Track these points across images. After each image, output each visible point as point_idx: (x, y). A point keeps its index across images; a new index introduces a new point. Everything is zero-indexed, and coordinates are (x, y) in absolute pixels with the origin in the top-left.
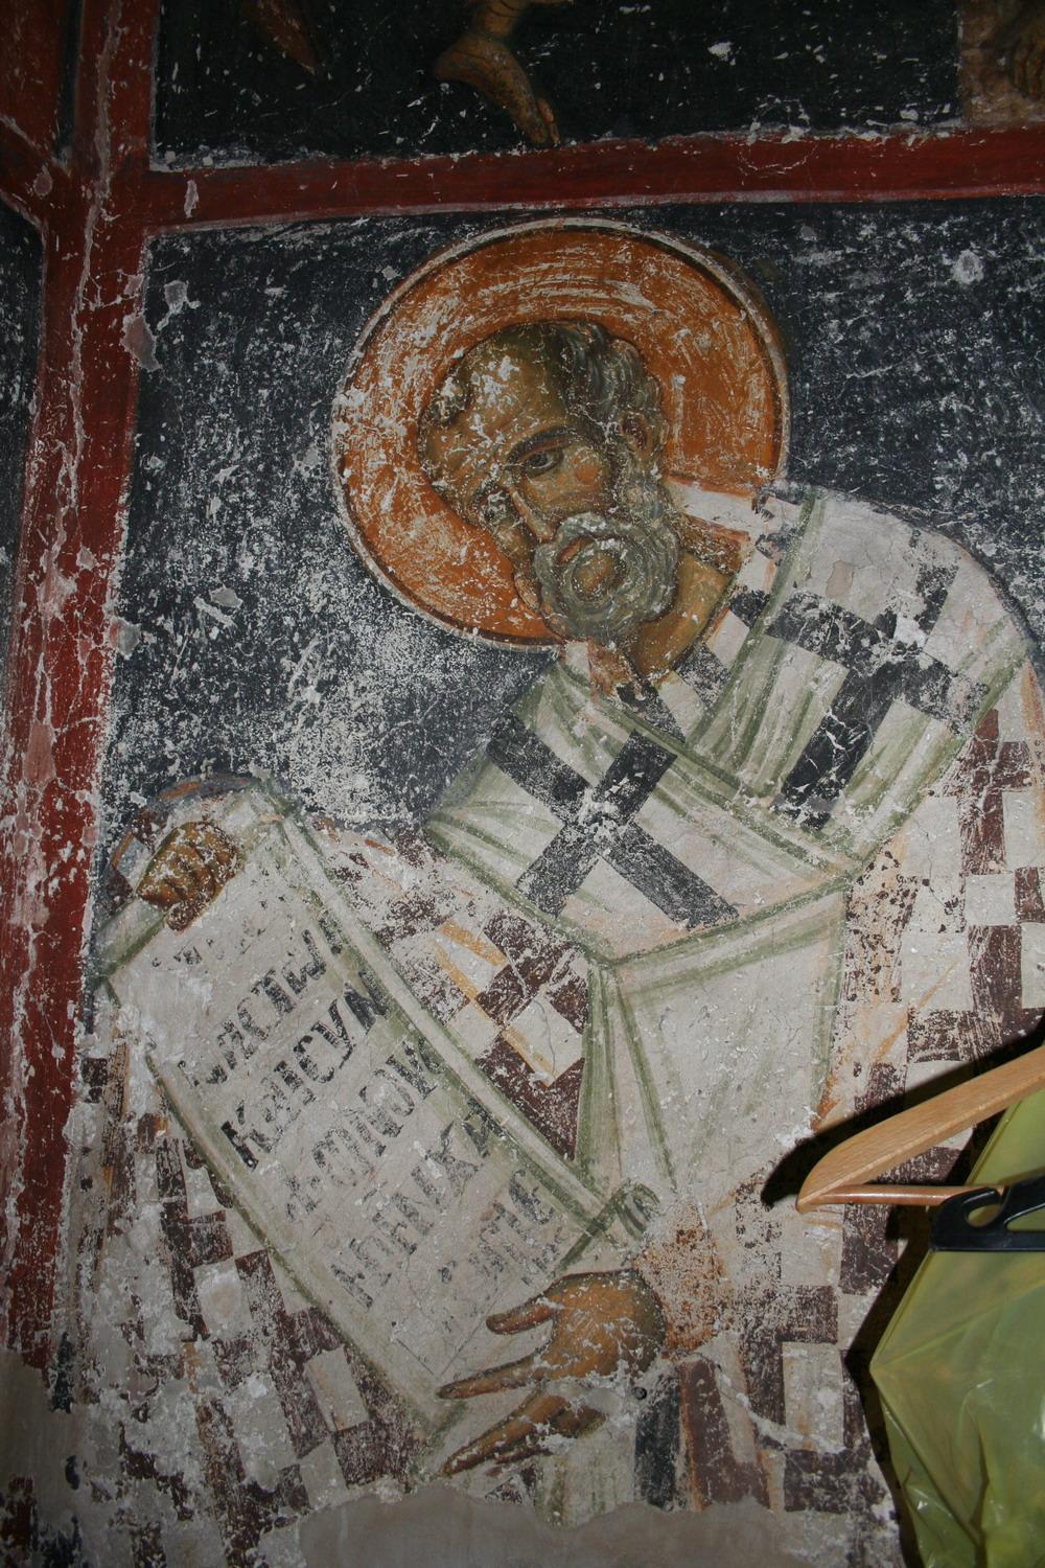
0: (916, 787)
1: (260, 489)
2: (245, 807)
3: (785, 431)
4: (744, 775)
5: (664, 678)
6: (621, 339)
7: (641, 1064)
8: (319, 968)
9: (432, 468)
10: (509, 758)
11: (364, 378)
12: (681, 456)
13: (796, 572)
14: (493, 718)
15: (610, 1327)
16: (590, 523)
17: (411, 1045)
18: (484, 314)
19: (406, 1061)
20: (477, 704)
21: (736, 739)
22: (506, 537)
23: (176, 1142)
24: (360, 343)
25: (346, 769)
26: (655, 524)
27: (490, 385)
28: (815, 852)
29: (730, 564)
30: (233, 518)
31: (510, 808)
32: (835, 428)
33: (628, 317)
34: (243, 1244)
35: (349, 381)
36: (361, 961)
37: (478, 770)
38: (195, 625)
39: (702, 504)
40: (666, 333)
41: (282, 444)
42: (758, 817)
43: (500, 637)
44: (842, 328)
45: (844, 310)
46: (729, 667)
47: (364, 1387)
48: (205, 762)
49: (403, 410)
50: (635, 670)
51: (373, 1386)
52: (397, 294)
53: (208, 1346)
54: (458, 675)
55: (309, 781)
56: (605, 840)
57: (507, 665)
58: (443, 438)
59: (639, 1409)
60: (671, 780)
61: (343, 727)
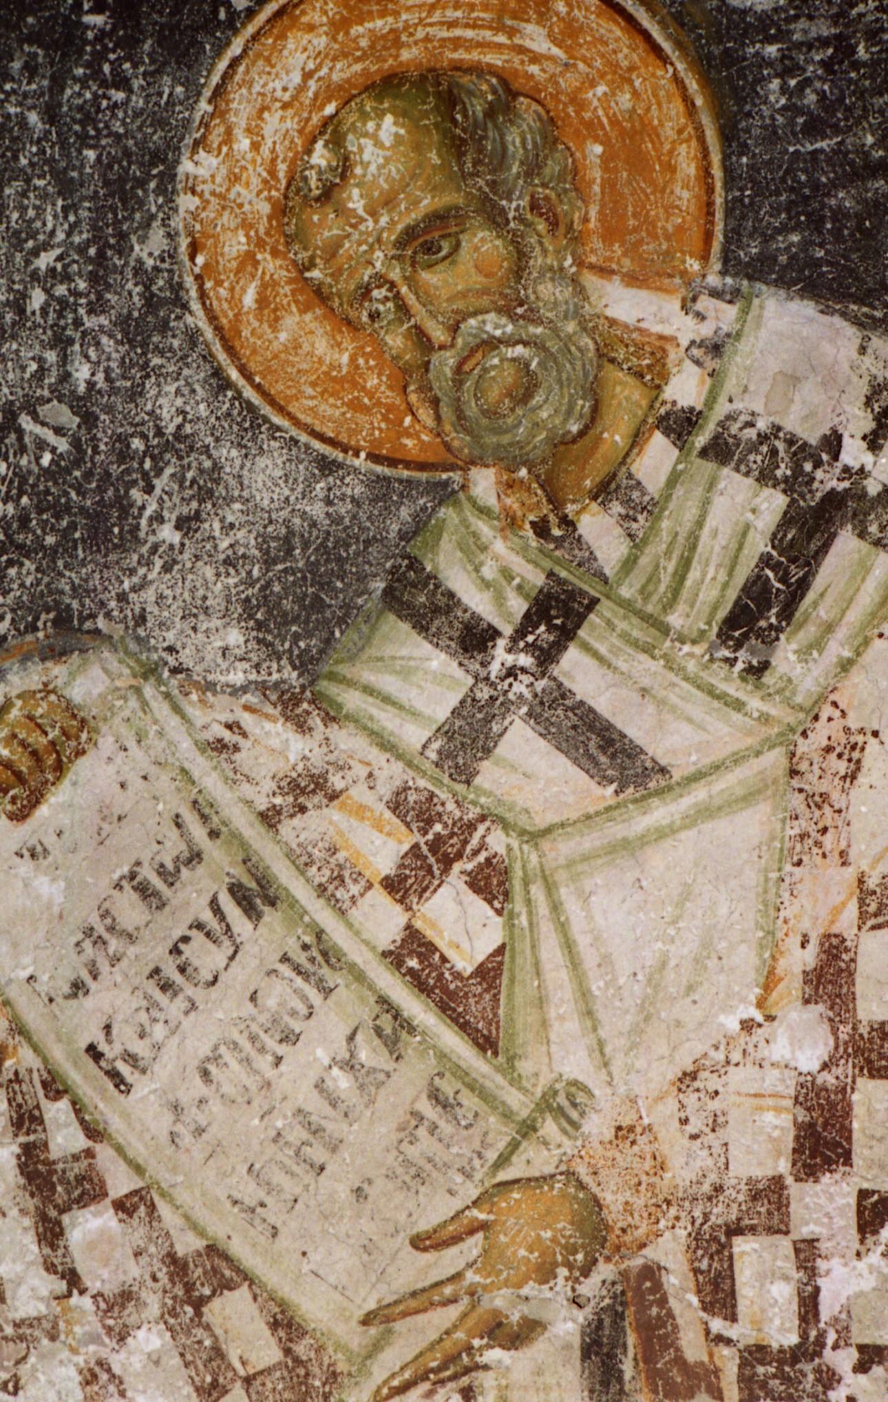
0: (863, 628)
1: (93, 279)
2: (96, 671)
3: (719, 215)
4: (675, 620)
5: (584, 509)
6: (527, 96)
7: (569, 946)
8: (195, 857)
9: (303, 256)
10: (409, 605)
11: (215, 138)
12: (597, 244)
13: (731, 385)
14: (388, 558)
15: (548, 1234)
16: (495, 325)
17: (307, 939)
18: (358, 60)
19: (301, 958)
20: (368, 543)
21: (666, 579)
22: (396, 341)
23: (30, 1071)
24: (207, 93)
25: (216, 622)
26: (571, 327)
27: (370, 153)
28: (755, 704)
29: (654, 374)
30: (60, 315)
31: (412, 663)
32: (775, 211)
33: (534, 69)
34: (120, 1183)
35: (196, 144)
36: (244, 845)
37: (373, 621)
38: (22, 449)
39: (624, 304)
40: (579, 89)
41: (117, 222)
42: (691, 666)
43: (392, 462)
44: (784, 89)
45: (787, 68)
46: (657, 497)
47: (275, 1325)
48: (43, 616)
49: (265, 182)
50: (550, 501)
51: (285, 1324)
52: (251, 29)
53: (86, 1302)
54: (344, 509)
55: (171, 636)
56: (521, 696)
57: (401, 495)
58: (316, 218)
59: (581, 1316)
60: (593, 627)
61: (209, 572)
